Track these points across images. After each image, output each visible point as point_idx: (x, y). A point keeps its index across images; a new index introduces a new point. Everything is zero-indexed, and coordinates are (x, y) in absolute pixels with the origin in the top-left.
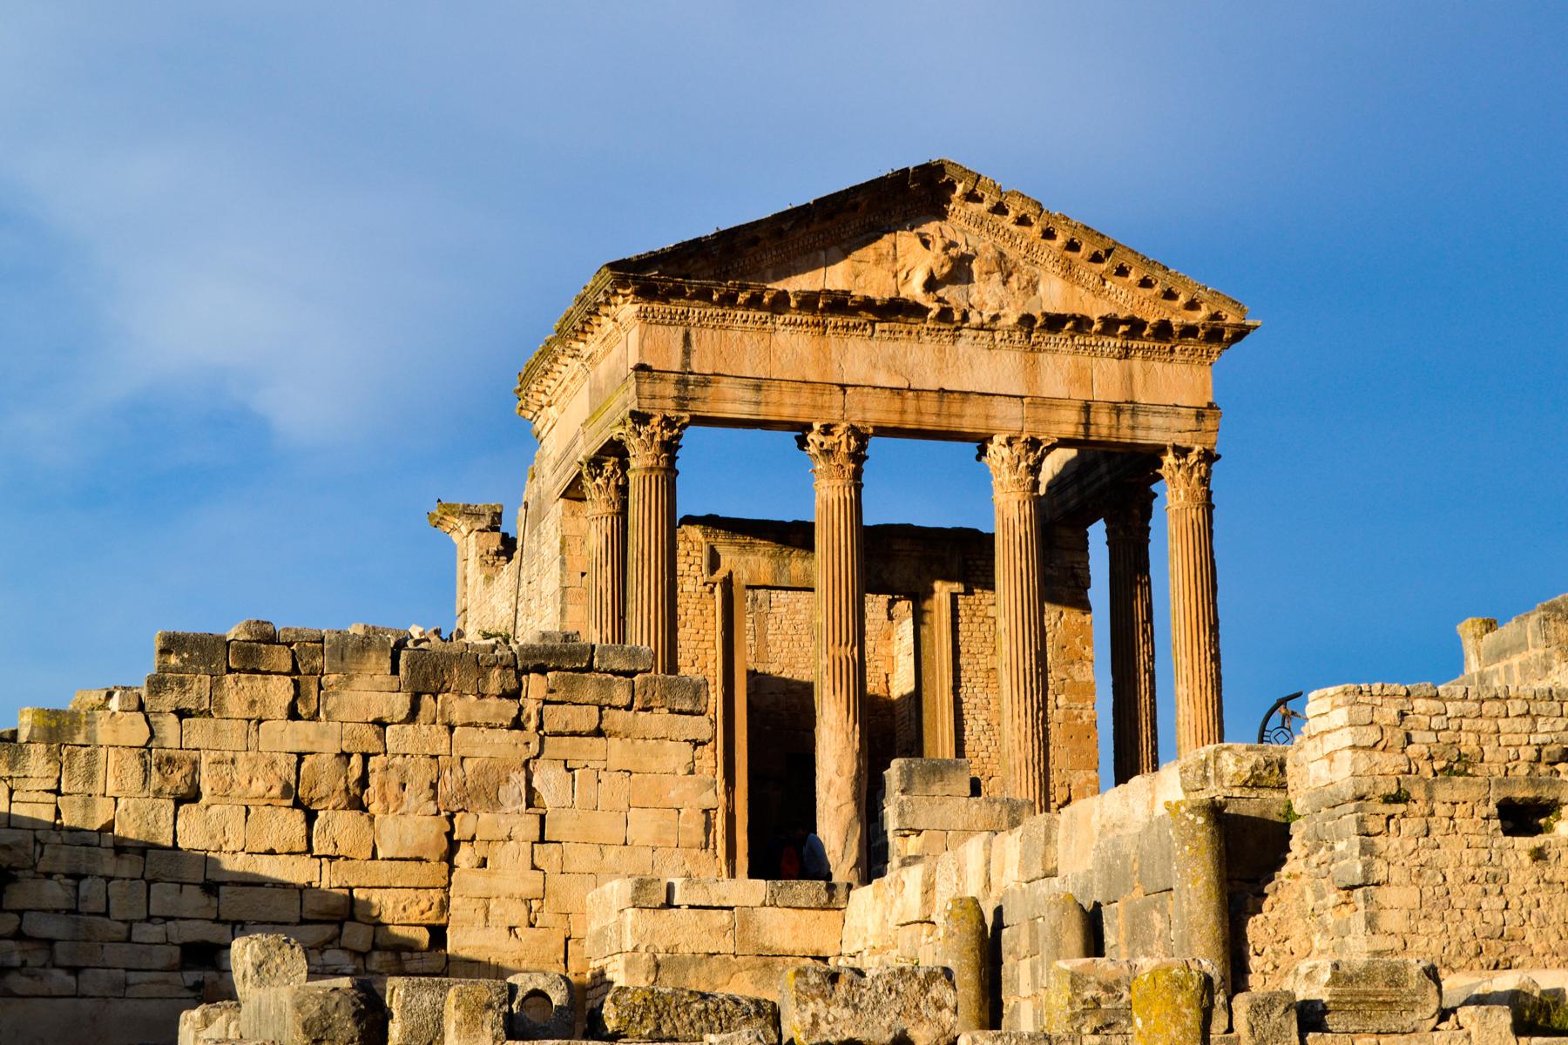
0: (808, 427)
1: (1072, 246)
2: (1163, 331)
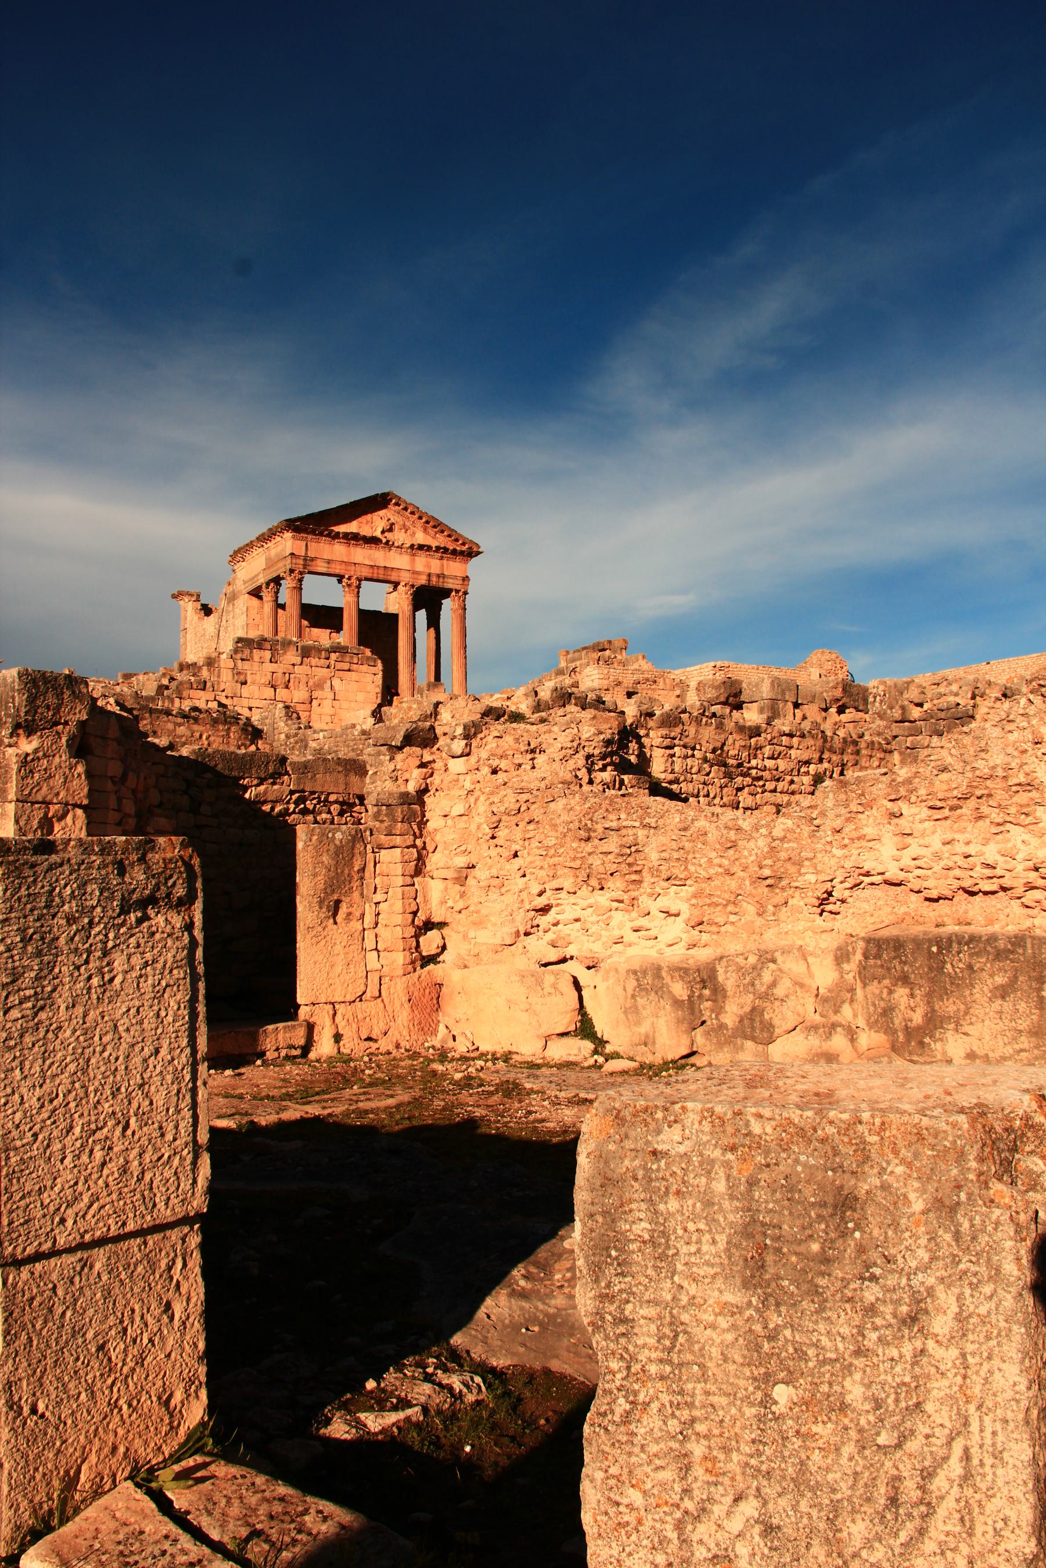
0: (343, 577)
1: (427, 522)
2: (454, 552)
